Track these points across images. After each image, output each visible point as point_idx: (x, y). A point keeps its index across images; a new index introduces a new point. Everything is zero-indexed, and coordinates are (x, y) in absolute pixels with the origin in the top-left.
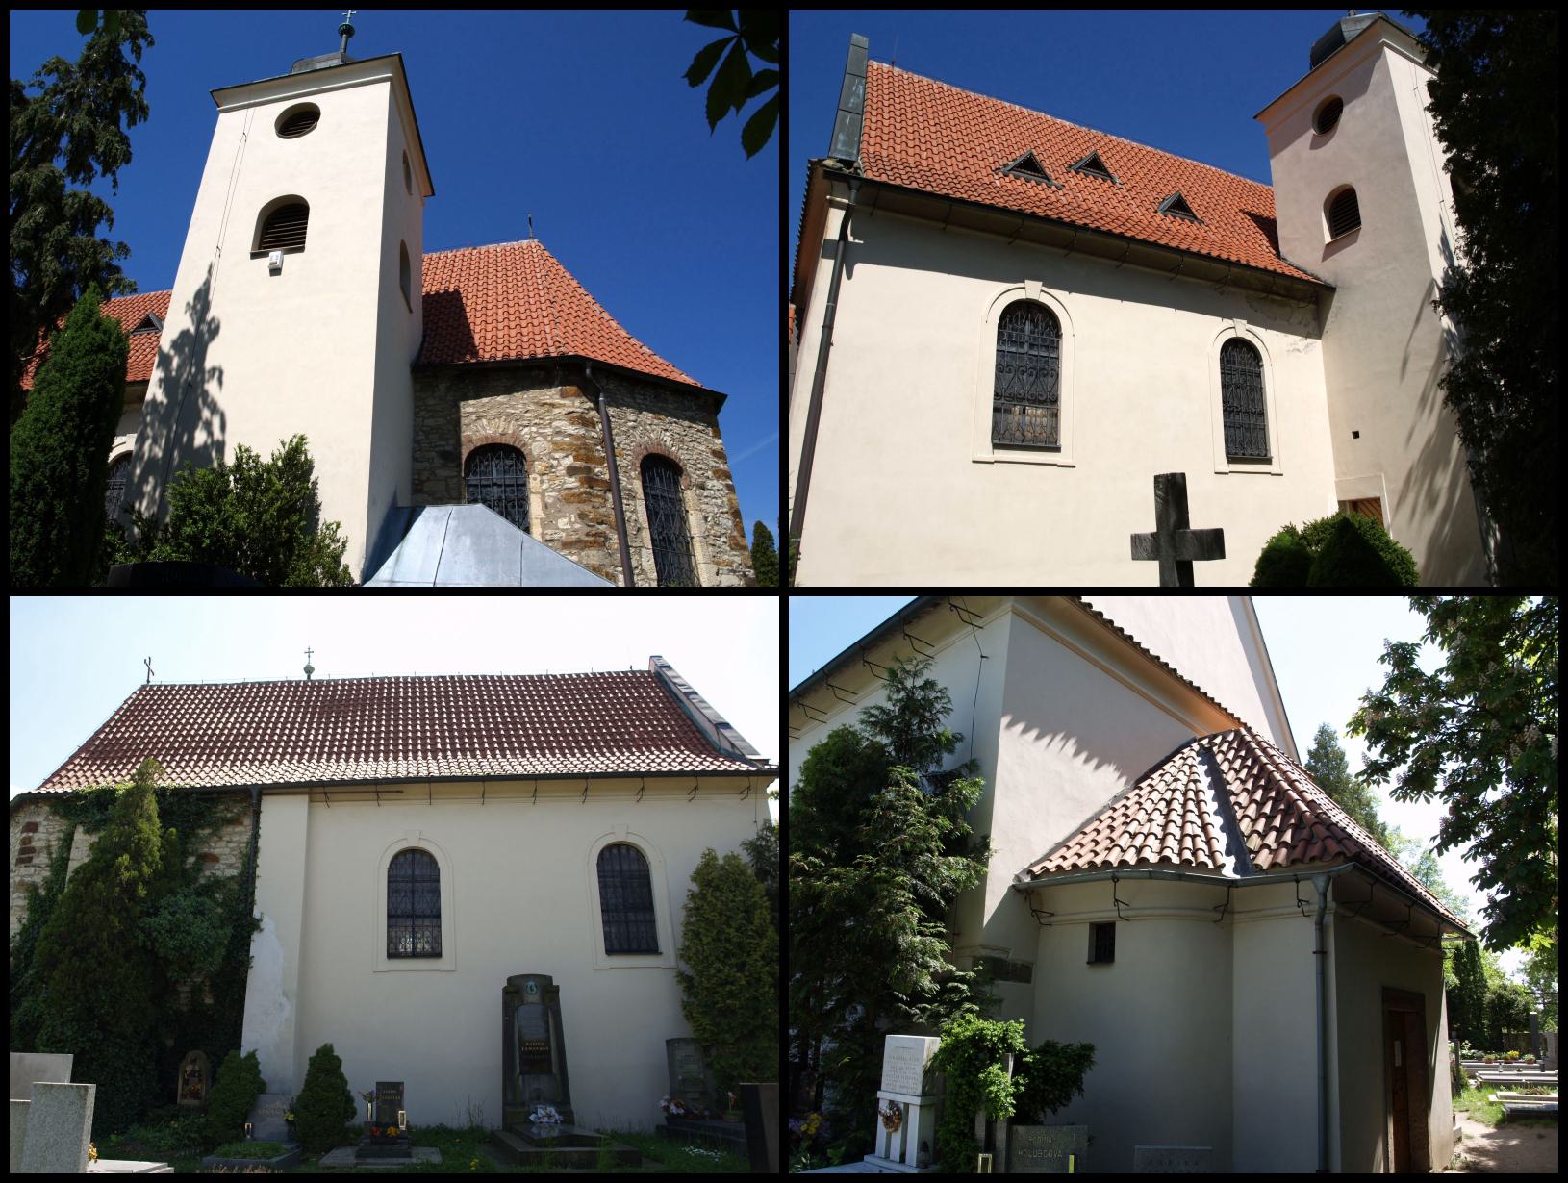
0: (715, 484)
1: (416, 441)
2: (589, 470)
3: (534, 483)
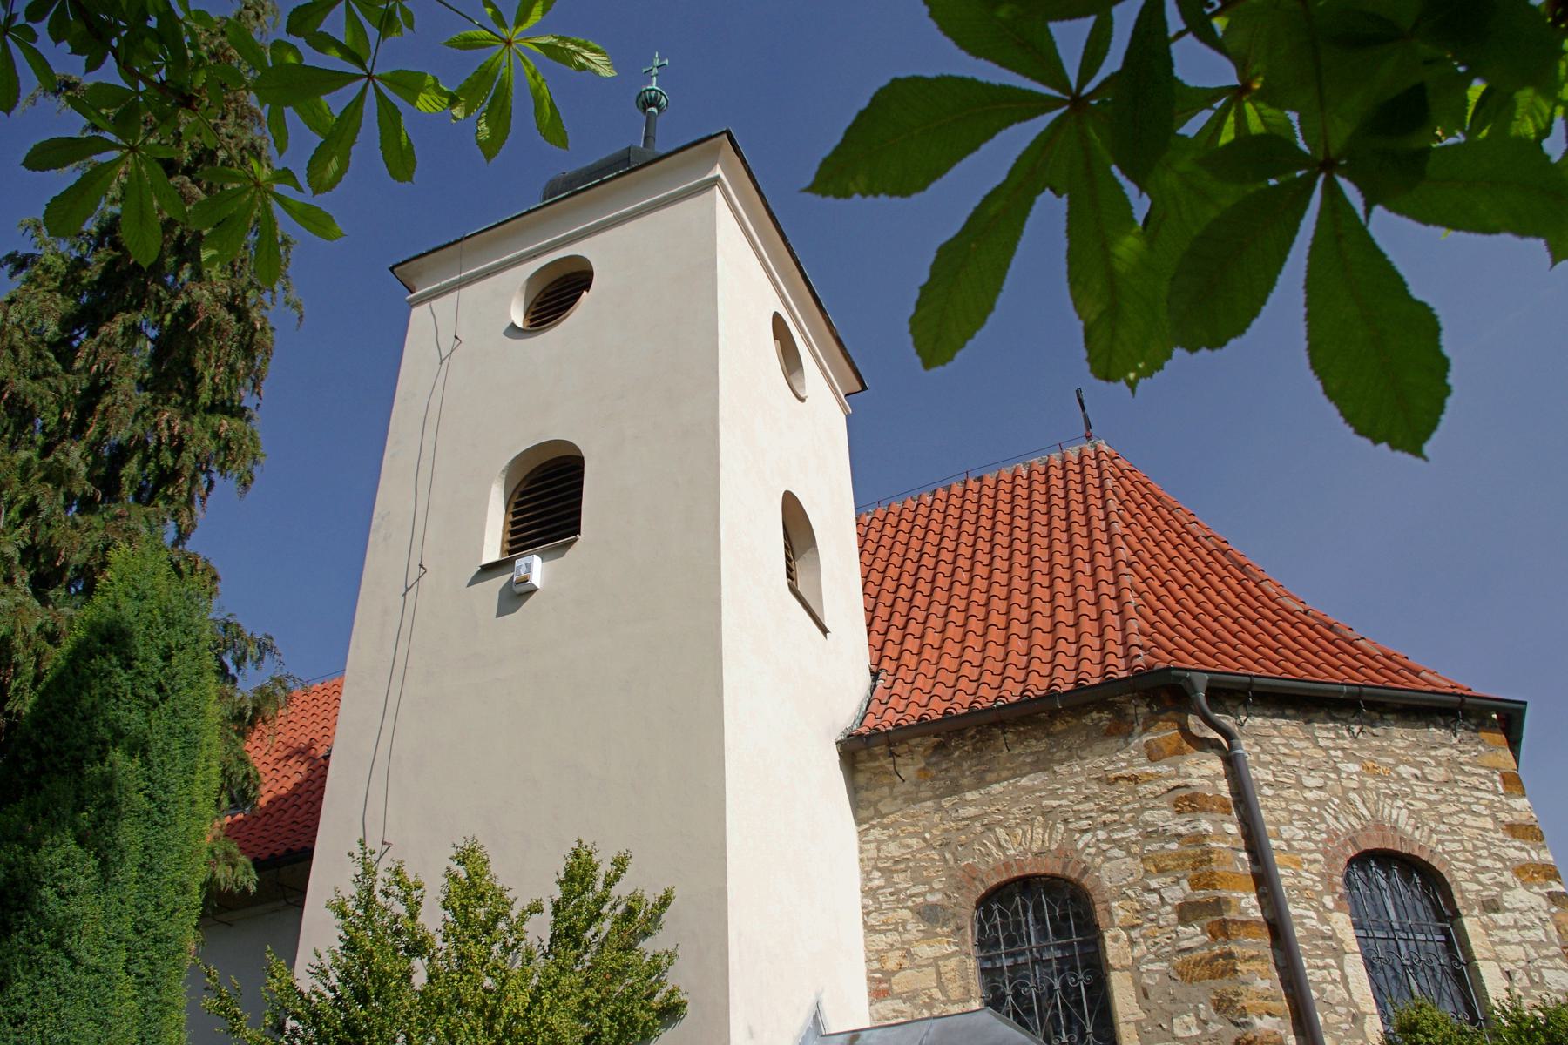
0: (1520, 897)
1: (869, 892)
2: (1218, 905)
3: (1115, 949)
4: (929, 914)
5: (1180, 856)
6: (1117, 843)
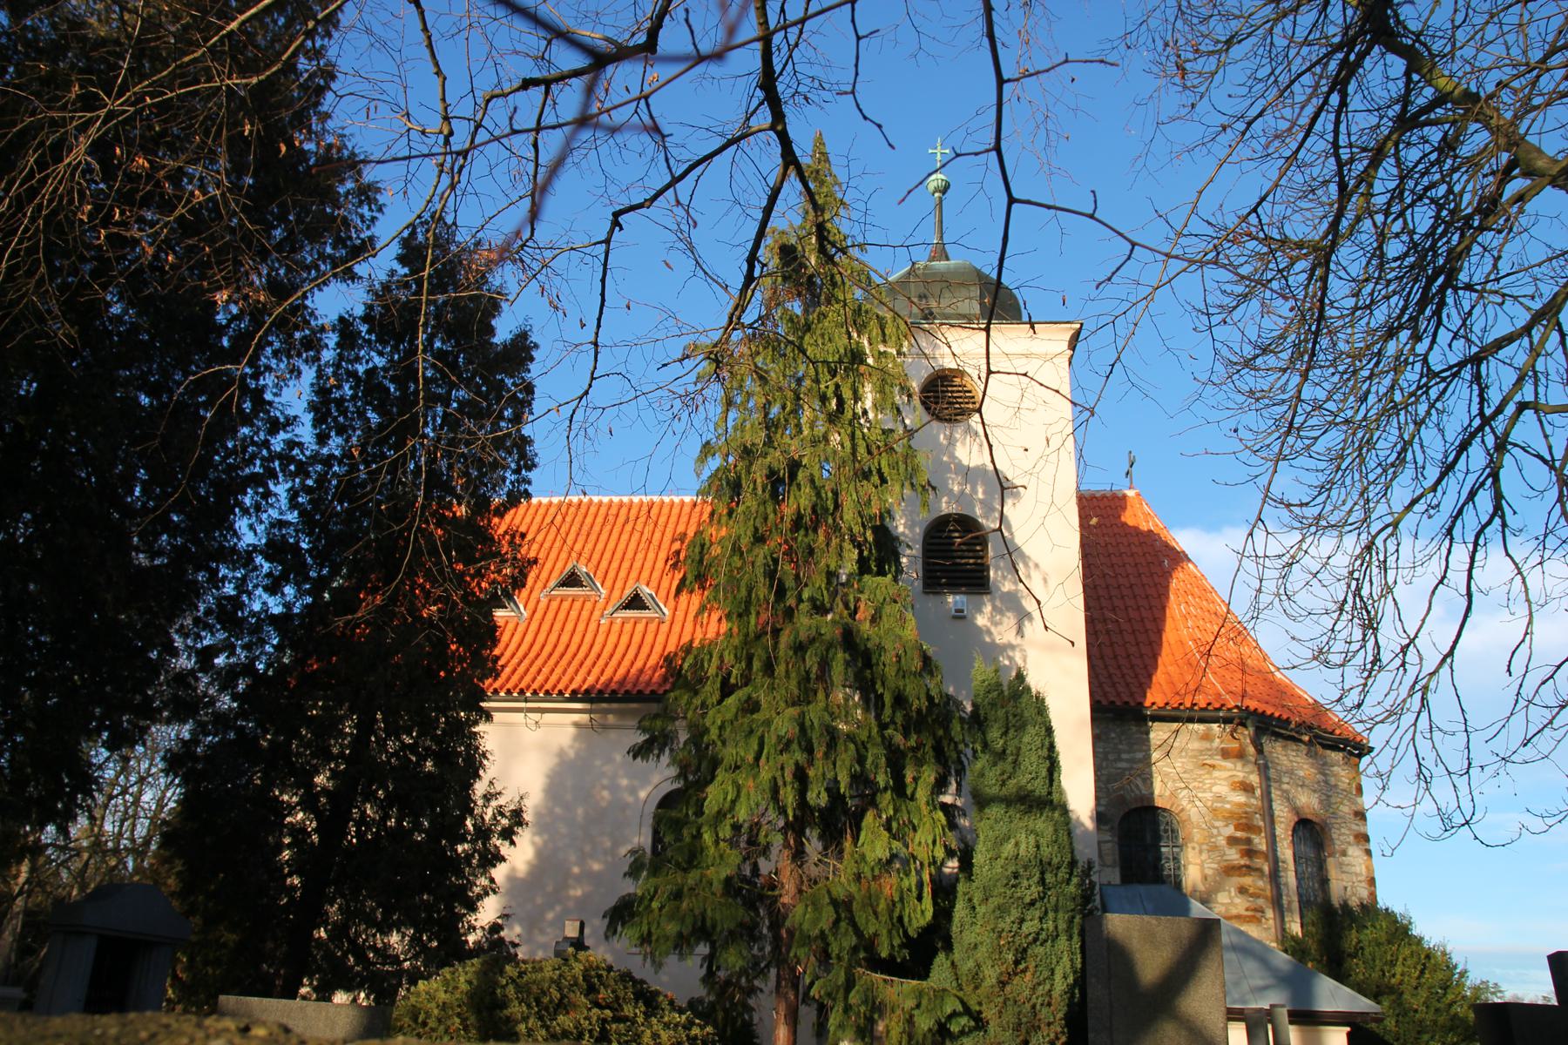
2: (1249, 841)
5: (1231, 812)
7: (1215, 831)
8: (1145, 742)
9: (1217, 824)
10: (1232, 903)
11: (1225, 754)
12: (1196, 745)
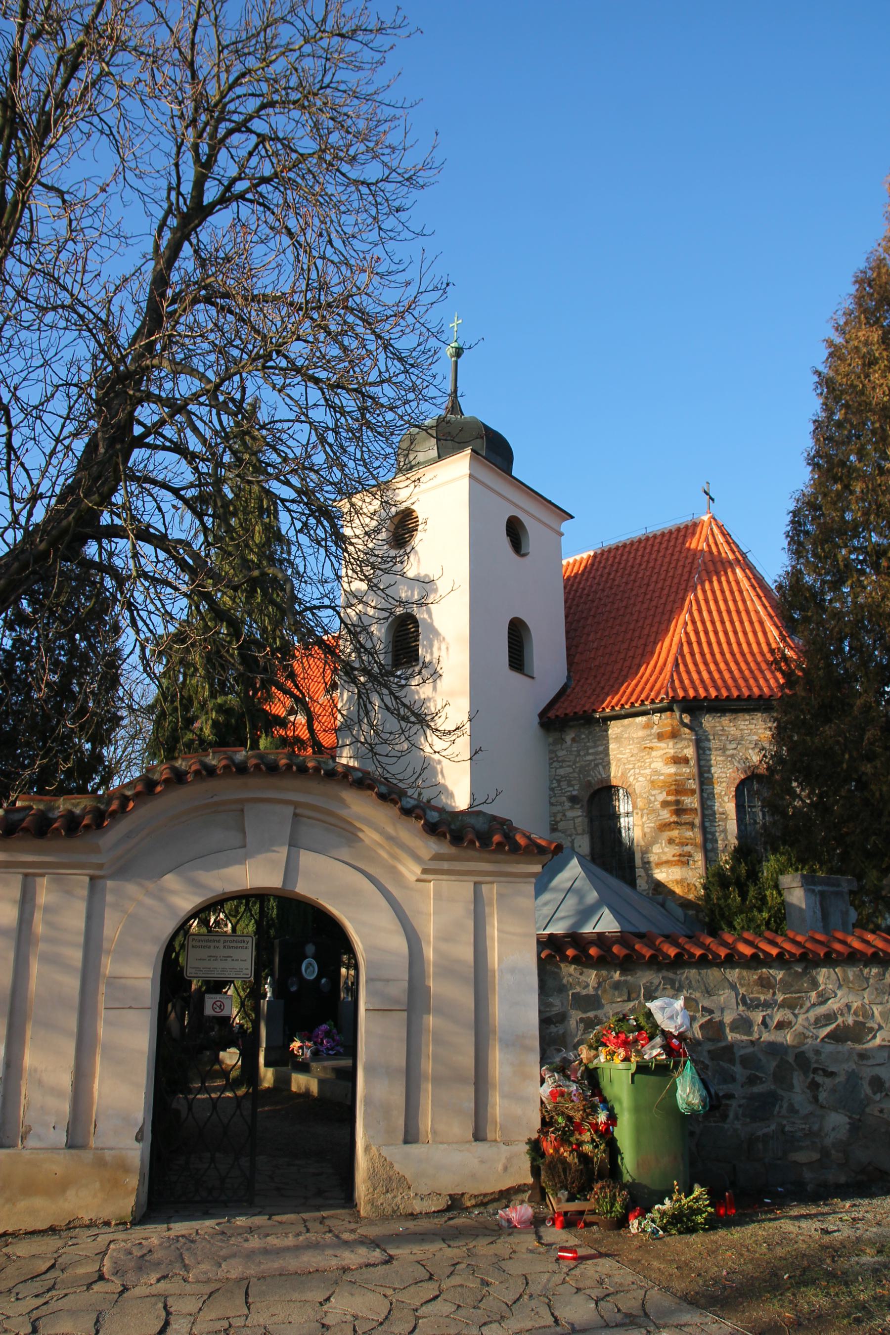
1: (552, 789)
4: (573, 800)
5: (664, 782)
6: (642, 775)
7: (652, 798)
8: (605, 739)
9: (654, 792)
10: (663, 853)
11: (660, 737)
12: (641, 733)
